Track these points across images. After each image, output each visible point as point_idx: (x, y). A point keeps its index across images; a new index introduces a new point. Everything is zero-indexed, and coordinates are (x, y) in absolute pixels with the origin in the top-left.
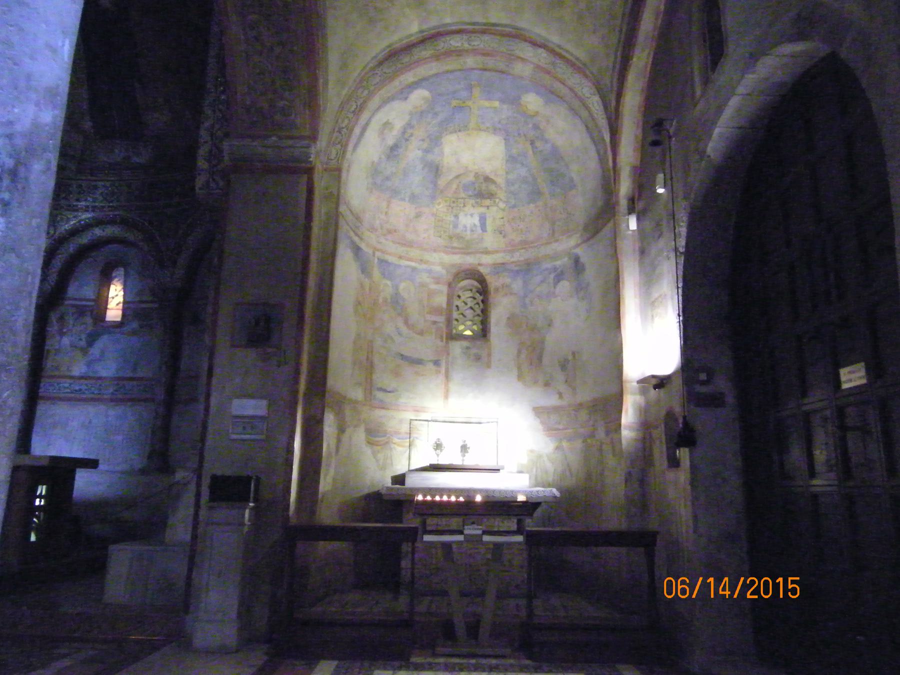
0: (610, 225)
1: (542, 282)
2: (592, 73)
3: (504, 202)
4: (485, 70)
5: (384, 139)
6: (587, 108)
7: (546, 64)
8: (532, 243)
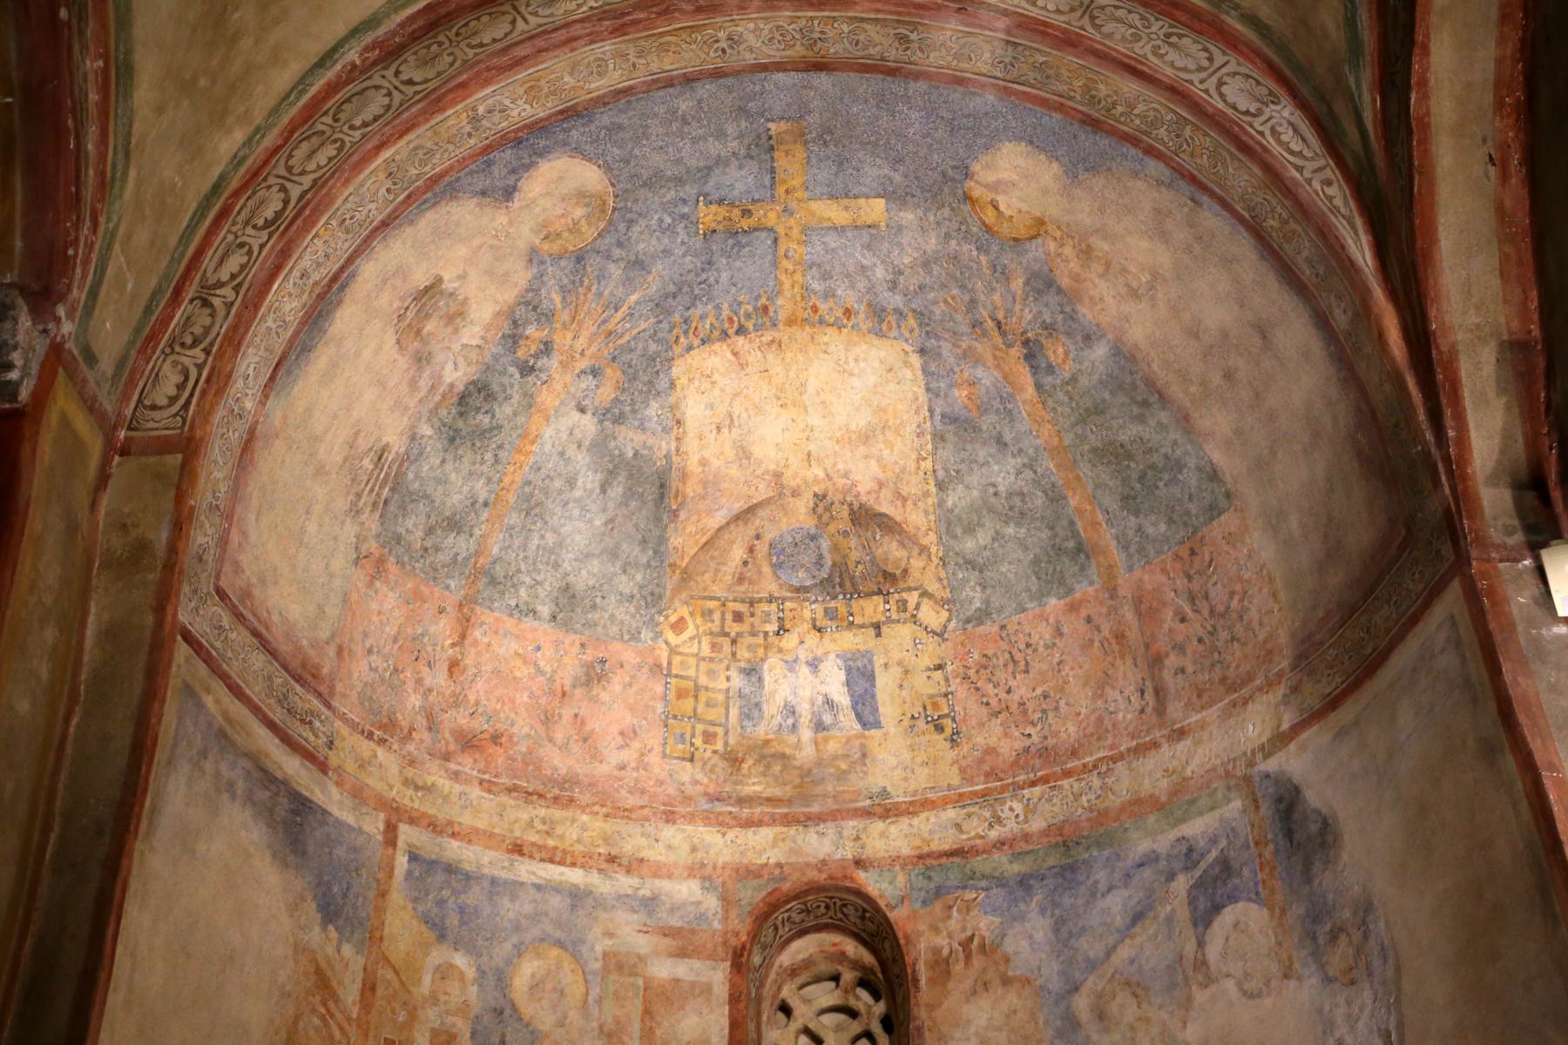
0: (1451, 601)
1: (1137, 918)
2: (1252, 20)
3: (943, 602)
4: (819, 67)
5: (421, 360)
6: (1248, 149)
7: (1058, 11)
8: (1074, 753)
